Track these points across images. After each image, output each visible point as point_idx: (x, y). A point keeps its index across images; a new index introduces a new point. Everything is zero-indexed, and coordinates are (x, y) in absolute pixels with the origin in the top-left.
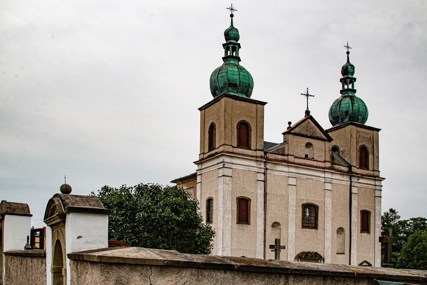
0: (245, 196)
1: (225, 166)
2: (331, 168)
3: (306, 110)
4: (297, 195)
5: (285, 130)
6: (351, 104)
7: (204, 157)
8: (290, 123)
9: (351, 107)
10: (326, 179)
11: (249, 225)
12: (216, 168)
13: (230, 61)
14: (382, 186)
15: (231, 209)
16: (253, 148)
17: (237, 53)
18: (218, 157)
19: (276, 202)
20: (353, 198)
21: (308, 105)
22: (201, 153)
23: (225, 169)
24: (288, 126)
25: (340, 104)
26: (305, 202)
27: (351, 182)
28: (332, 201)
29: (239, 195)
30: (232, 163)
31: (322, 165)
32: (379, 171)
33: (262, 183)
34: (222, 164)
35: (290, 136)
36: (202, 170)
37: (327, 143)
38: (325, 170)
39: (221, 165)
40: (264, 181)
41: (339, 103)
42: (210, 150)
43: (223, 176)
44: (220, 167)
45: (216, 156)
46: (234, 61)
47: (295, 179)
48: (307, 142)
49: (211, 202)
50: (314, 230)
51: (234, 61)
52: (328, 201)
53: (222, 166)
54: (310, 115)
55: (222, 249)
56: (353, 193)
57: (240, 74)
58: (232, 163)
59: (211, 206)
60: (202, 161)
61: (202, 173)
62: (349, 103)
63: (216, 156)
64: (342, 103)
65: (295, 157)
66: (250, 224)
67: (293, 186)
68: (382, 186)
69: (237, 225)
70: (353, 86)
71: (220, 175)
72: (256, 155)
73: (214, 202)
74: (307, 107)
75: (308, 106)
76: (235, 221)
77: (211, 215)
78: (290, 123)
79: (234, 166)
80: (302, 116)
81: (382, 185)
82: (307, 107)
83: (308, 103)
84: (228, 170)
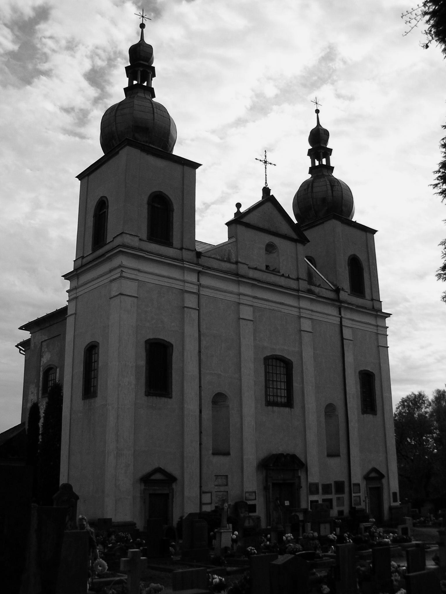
0: (161, 337)
1: (124, 274)
2: (310, 292)
3: (264, 187)
5: (231, 217)
6: (329, 187)
7: (83, 264)
8: (239, 205)
9: (330, 191)
10: (301, 310)
11: (169, 400)
12: (106, 281)
13: (138, 93)
14: (388, 327)
15: (117, 407)
16: (176, 242)
17: (149, 83)
18: (110, 258)
19: (219, 352)
20: (346, 348)
21: (266, 178)
22: (77, 258)
23: (123, 281)
24: (236, 210)
25: (312, 187)
26: (268, 353)
27: (341, 318)
29: (151, 336)
30: (139, 271)
32: (381, 302)
33: (197, 312)
34: (119, 270)
35: (241, 229)
36: (78, 290)
37: (300, 247)
38: (300, 294)
39: (116, 274)
40: (199, 310)
41: (310, 185)
42: (94, 250)
43: (121, 294)
44: (114, 277)
45: (107, 256)
46: (144, 94)
47: (252, 309)
48: (267, 242)
49: (94, 353)
51: (143, 94)
52: (308, 354)
53: (119, 275)
54: (271, 194)
55: (115, 452)
56: (346, 339)
57: (155, 111)
58: (139, 271)
59: (95, 362)
60: (79, 272)
61: (78, 295)
62: (326, 185)
63: (107, 256)
64: (315, 184)
65: (249, 268)
66: (171, 398)
67: (249, 322)
68: (388, 327)
69: (146, 398)
70: (328, 161)
71: (114, 293)
72: (182, 258)
74: (266, 183)
75: (266, 180)
76: (143, 390)
78: (239, 205)
79: (141, 277)
80: (258, 197)
81: (387, 326)
82: (266, 183)
83: (266, 175)
84: (129, 282)
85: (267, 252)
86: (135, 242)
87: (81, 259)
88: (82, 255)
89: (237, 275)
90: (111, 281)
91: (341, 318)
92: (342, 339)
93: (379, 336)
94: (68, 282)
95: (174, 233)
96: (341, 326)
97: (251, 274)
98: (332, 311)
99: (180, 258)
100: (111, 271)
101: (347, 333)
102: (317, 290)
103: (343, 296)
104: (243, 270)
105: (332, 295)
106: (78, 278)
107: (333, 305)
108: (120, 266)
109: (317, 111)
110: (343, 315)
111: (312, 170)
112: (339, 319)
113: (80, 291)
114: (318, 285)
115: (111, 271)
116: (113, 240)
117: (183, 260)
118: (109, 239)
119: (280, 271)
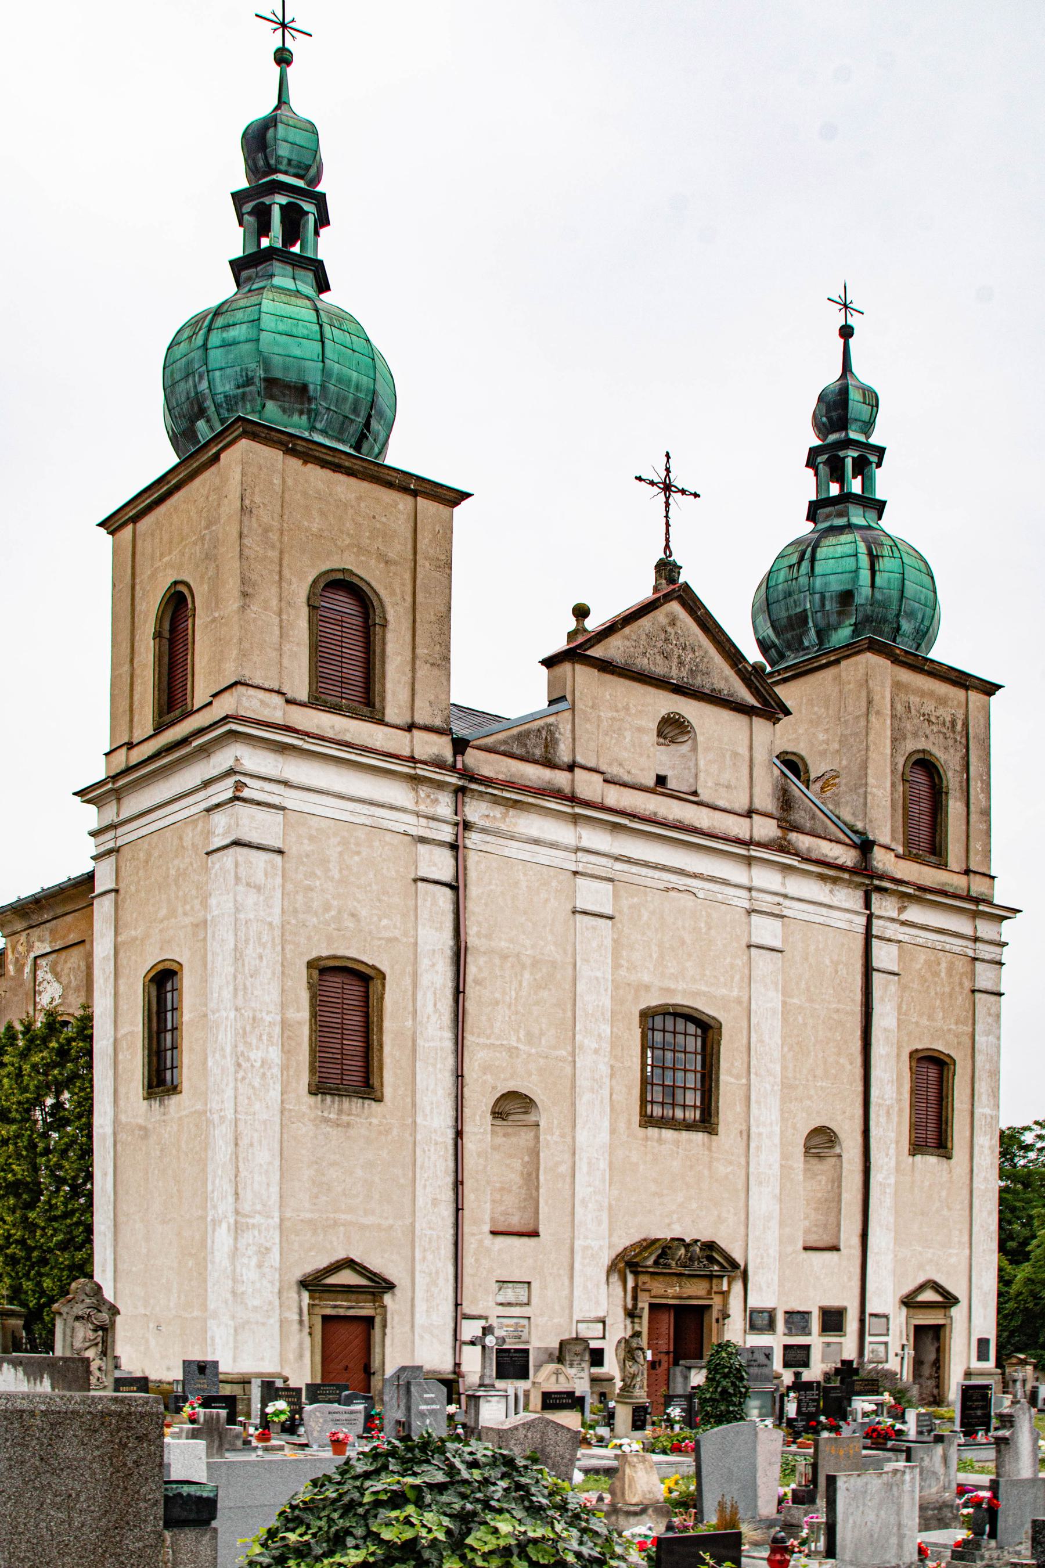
1: (246, 793)
2: (783, 847)
4: (616, 966)
5: (559, 644)
6: (864, 561)
8: (581, 612)
9: (865, 575)
12: (194, 810)
18: (205, 751)
24: (572, 624)
25: (813, 560)
28: (784, 1003)
30: (286, 783)
31: (738, 827)
34: (230, 781)
35: (583, 677)
37: (760, 725)
39: (223, 791)
40: (454, 888)
41: (807, 555)
42: (160, 728)
43: (237, 843)
44: (215, 800)
48: (663, 712)
50: (699, 1137)
53: (229, 794)
54: (681, 580)
58: (286, 783)
63: (195, 744)
64: (821, 553)
65: (606, 781)
72: (412, 751)
73: (188, 982)
74: (667, 546)
77: (169, 1053)
78: (581, 612)
79: (292, 799)
82: (667, 546)
85: (662, 740)
86: (274, 710)
87: (124, 750)
88: (126, 740)
89: (573, 799)
90: (208, 810)
91: (870, 918)
92: (868, 970)
93: (978, 964)
94: (92, 808)
95: (389, 686)
96: (868, 936)
97: (614, 797)
98: (849, 898)
99: (406, 753)
100: (206, 784)
101: (884, 956)
102: (803, 842)
103: (882, 860)
104: (588, 786)
105: (847, 857)
106: (119, 800)
107: (849, 883)
108: (231, 772)
109: (846, 332)
110: (875, 909)
111: (814, 511)
112: (863, 920)
113: (126, 835)
114: (797, 816)
115: (206, 784)
116: (210, 703)
117: (413, 758)
118: (200, 697)
119: (699, 791)
